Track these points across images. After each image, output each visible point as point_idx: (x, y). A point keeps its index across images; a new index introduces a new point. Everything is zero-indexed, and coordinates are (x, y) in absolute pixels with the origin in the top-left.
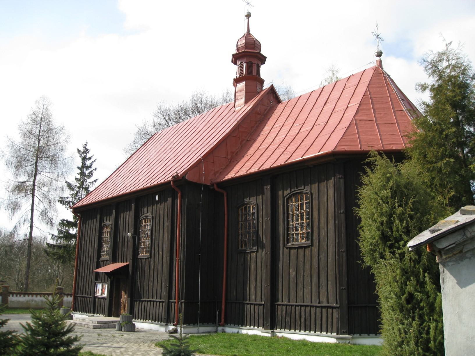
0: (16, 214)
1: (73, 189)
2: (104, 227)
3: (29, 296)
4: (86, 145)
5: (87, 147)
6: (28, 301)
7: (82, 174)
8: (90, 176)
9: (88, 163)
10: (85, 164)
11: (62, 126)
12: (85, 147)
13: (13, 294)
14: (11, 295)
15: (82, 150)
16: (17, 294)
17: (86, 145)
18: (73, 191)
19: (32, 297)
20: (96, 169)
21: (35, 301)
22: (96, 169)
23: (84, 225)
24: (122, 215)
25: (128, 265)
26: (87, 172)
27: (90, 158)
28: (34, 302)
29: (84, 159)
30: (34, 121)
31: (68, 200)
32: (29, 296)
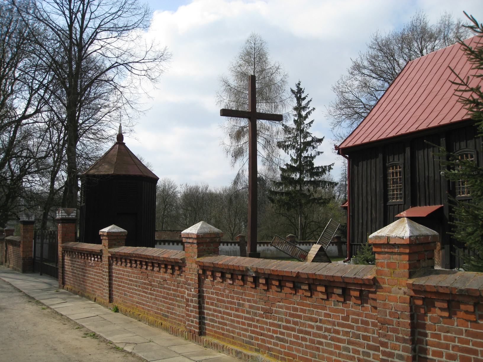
0: (238, 161)
1: (290, 132)
2: (389, 167)
3: (264, 246)
4: (299, 84)
5: (301, 87)
6: (264, 251)
7: (300, 116)
8: (306, 117)
9: (304, 103)
10: (301, 105)
11: (277, 65)
12: (298, 87)
13: (224, 243)
14: (221, 244)
15: (295, 89)
16: (227, 243)
17: (299, 84)
18: (290, 134)
19: (267, 246)
20: (314, 109)
21: (271, 250)
22: (314, 109)
23: (355, 167)
24: (420, 155)
25: (441, 209)
26: (304, 113)
27: (304, 98)
28: (269, 252)
29: (299, 99)
30: (402, 36)
31: (287, 144)
32: (264, 246)
